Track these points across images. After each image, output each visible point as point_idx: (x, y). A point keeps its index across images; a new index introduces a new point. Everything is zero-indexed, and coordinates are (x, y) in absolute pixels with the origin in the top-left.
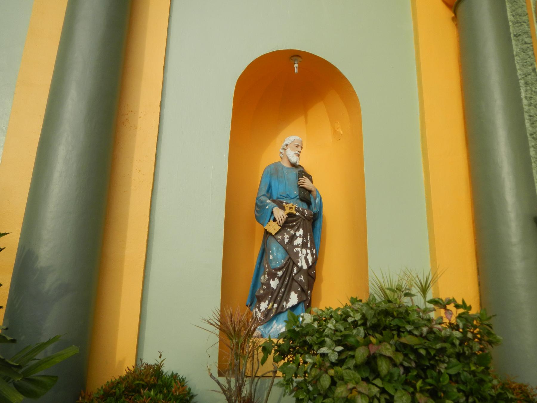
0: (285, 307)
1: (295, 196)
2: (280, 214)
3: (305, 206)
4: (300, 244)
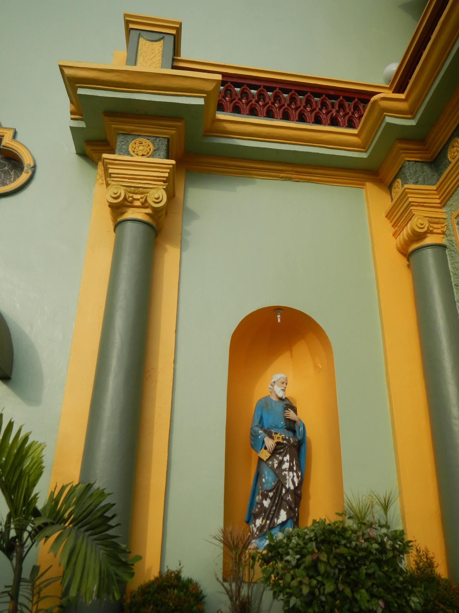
0: (276, 523)
1: (282, 426)
2: (270, 443)
3: (291, 434)
4: (287, 468)
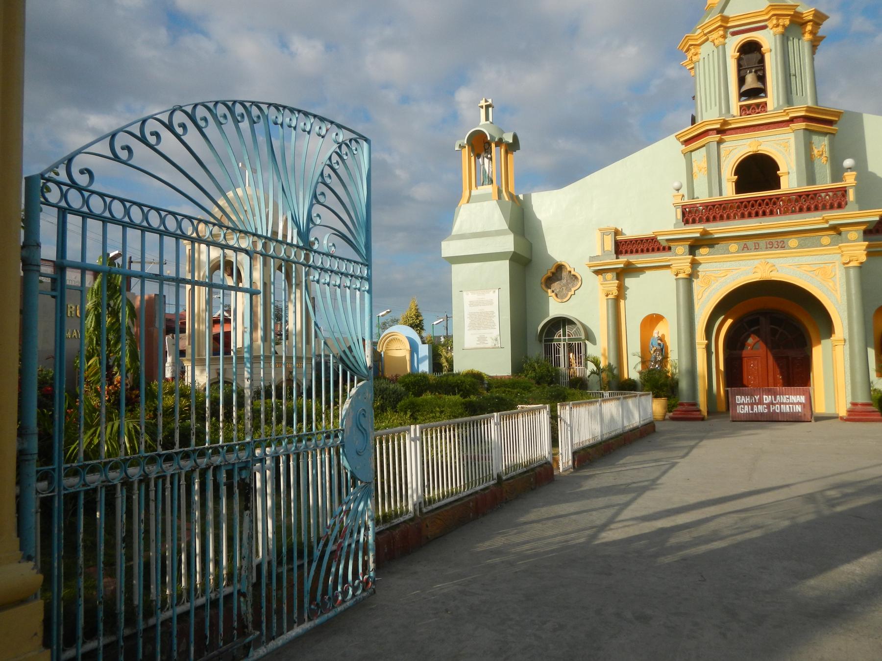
2: (653, 349)
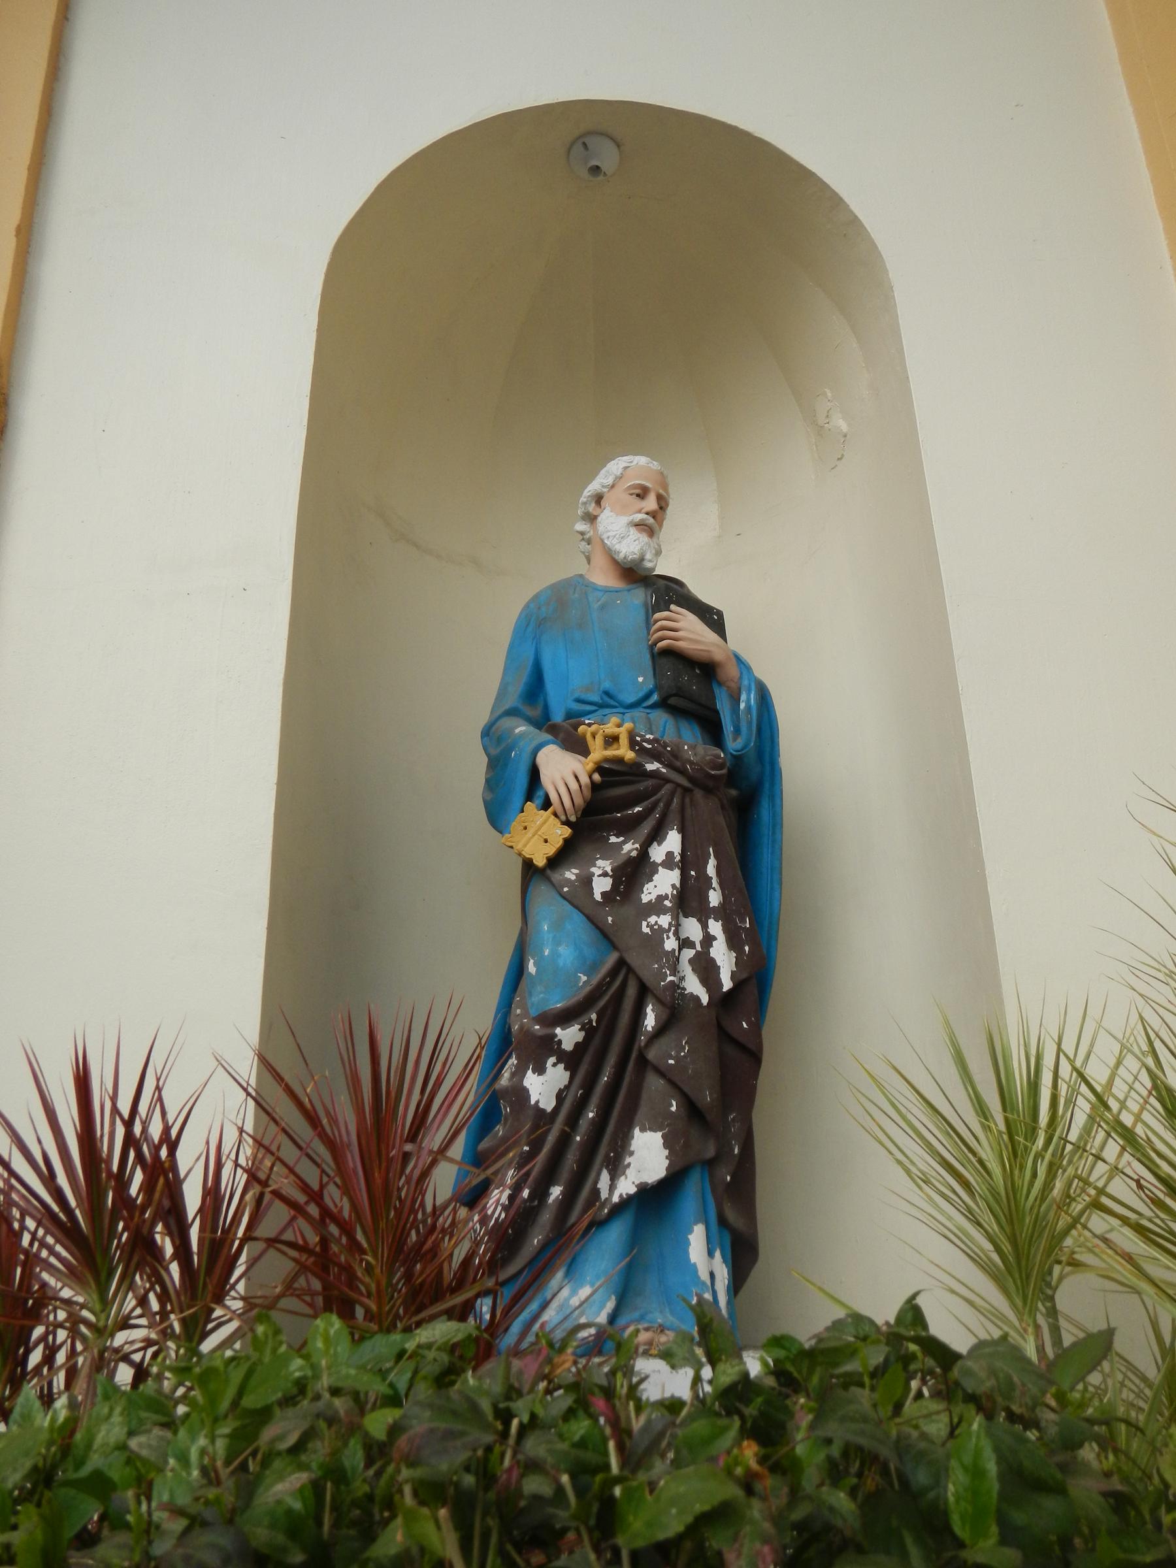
0: (604, 1195)
1: (641, 695)
4: (666, 897)
